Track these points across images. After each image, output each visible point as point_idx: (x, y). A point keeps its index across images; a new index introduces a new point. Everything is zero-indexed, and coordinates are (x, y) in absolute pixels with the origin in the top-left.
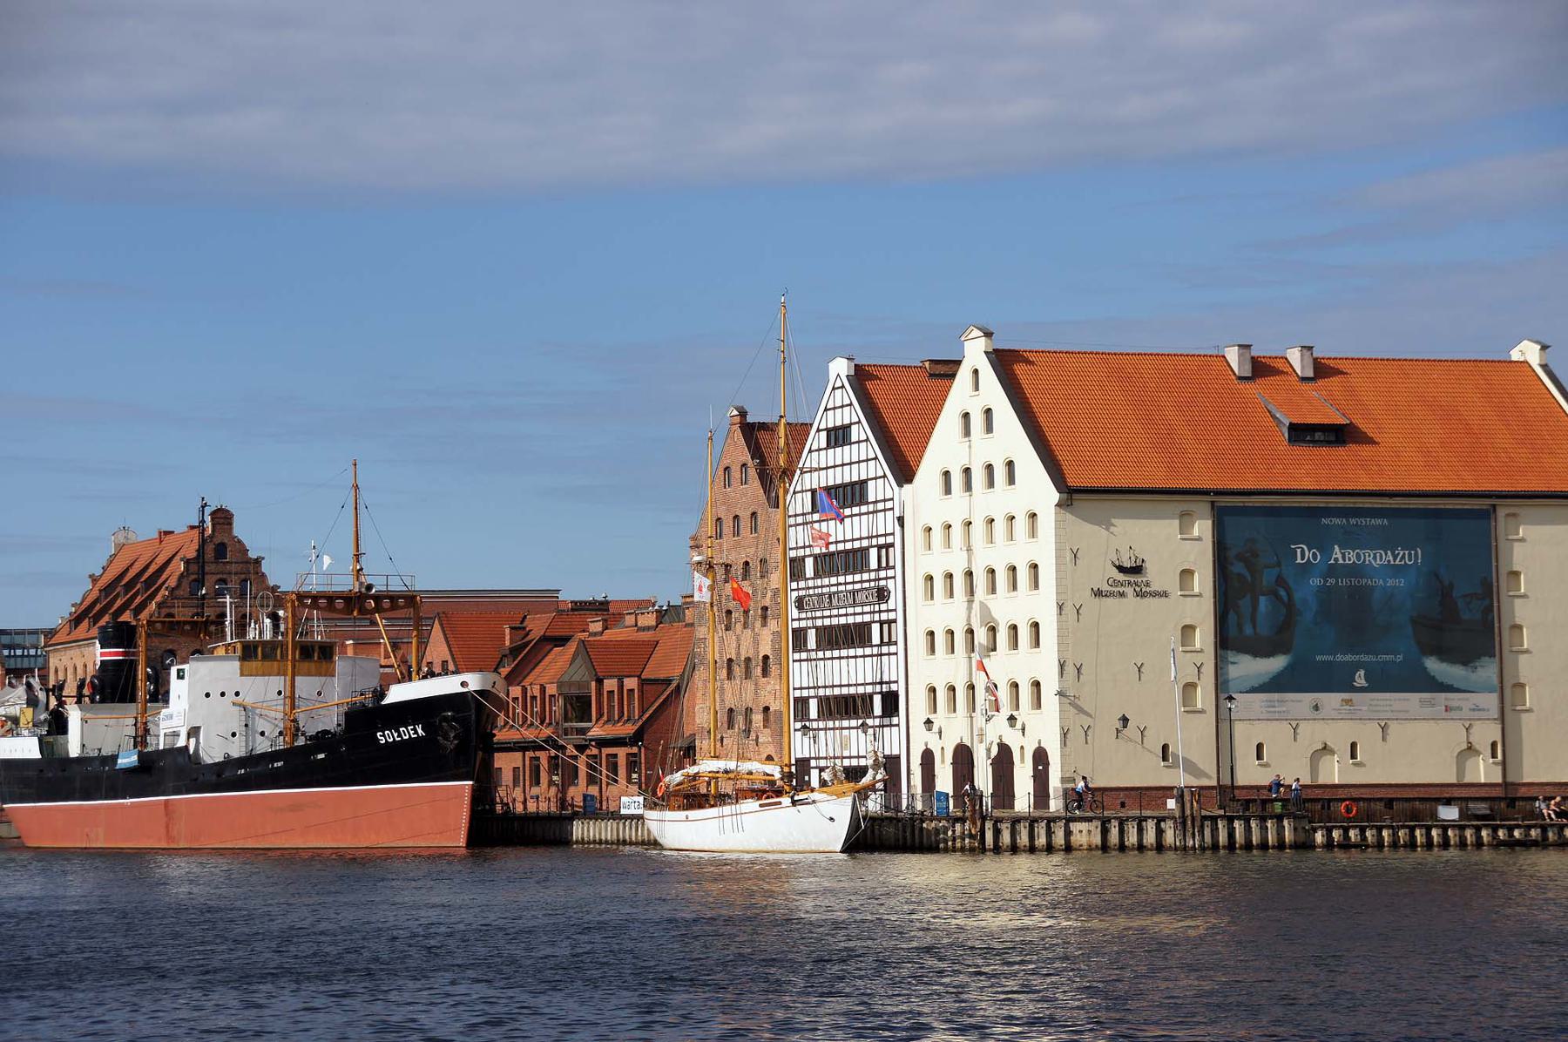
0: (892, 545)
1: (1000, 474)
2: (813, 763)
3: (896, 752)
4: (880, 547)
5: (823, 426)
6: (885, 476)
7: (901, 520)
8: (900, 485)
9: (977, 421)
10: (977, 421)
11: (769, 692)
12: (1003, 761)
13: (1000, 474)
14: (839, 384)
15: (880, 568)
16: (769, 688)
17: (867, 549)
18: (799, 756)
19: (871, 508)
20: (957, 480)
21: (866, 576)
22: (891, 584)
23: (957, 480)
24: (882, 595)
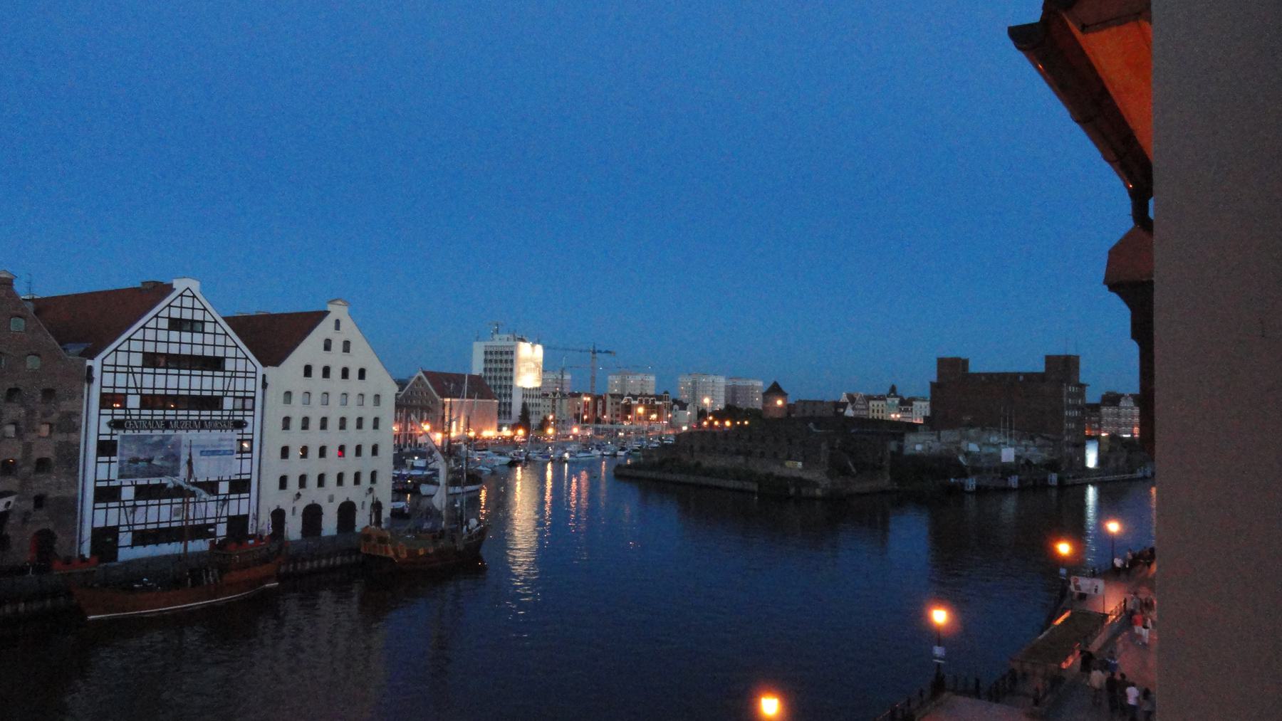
0: (254, 398)
1: (354, 374)
2: (121, 529)
3: (243, 512)
4: (235, 397)
5: (165, 313)
6: (247, 358)
7: (265, 385)
8: (264, 365)
9: (337, 346)
10: (337, 346)
11: (48, 484)
12: (347, 511)
13: (354, 374)
14: (188, 293)
15: (234, 410)
16: (48, 481)
17: (222, 397)
18: (99, 523)
19: (228, 374)
20: (317, 372)
21: (219, 413)
22: (248, 419)
23: (317, 372)
24: (240, 425)
